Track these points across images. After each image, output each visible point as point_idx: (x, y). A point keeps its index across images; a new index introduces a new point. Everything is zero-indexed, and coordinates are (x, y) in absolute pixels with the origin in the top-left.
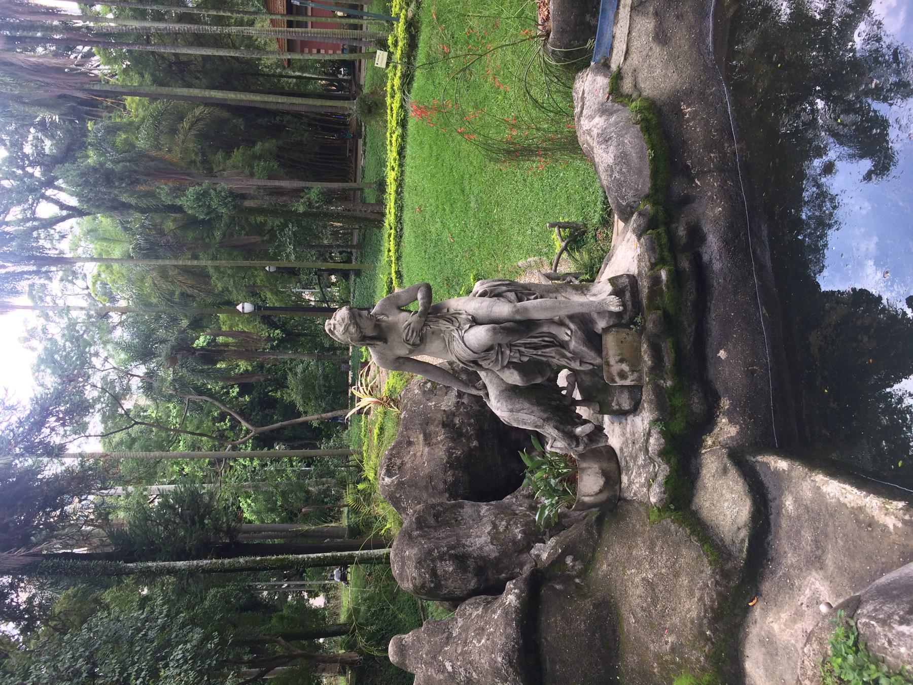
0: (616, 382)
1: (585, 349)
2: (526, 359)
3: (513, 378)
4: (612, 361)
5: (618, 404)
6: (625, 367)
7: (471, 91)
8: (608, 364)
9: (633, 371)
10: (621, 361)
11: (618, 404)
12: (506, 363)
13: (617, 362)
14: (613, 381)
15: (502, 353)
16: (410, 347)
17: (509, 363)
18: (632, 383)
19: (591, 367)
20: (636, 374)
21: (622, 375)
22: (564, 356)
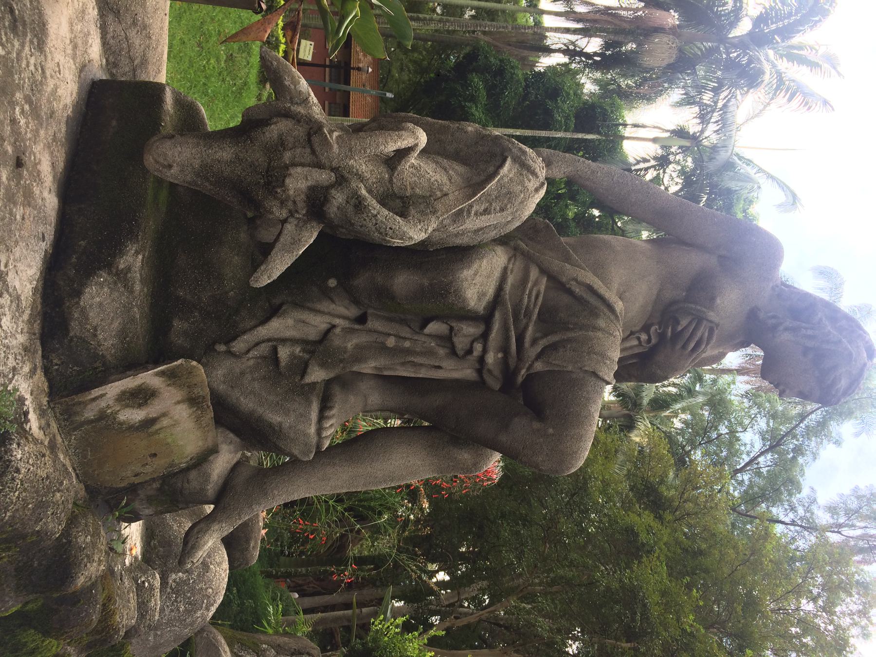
0: (162, 374)
1: (275, 418)
2: (433, 327)
3: (477, 282)
4: (182, 413)
5: (122, 277)
6: (134, 415)
7: (198, 23)
8: (193, 401)
9: (102, 416)
10: (149, 423)
11: (122, 277)
12: (496, 326)
13: (164, 415)
14: (171, 376)
15: (505, 349)
16: (712, 315)
17: (486, 319)
18: (96, 392)
19: (238, 346)
20: (90, 413)
21: (141, 396)
22: (318, 348)
